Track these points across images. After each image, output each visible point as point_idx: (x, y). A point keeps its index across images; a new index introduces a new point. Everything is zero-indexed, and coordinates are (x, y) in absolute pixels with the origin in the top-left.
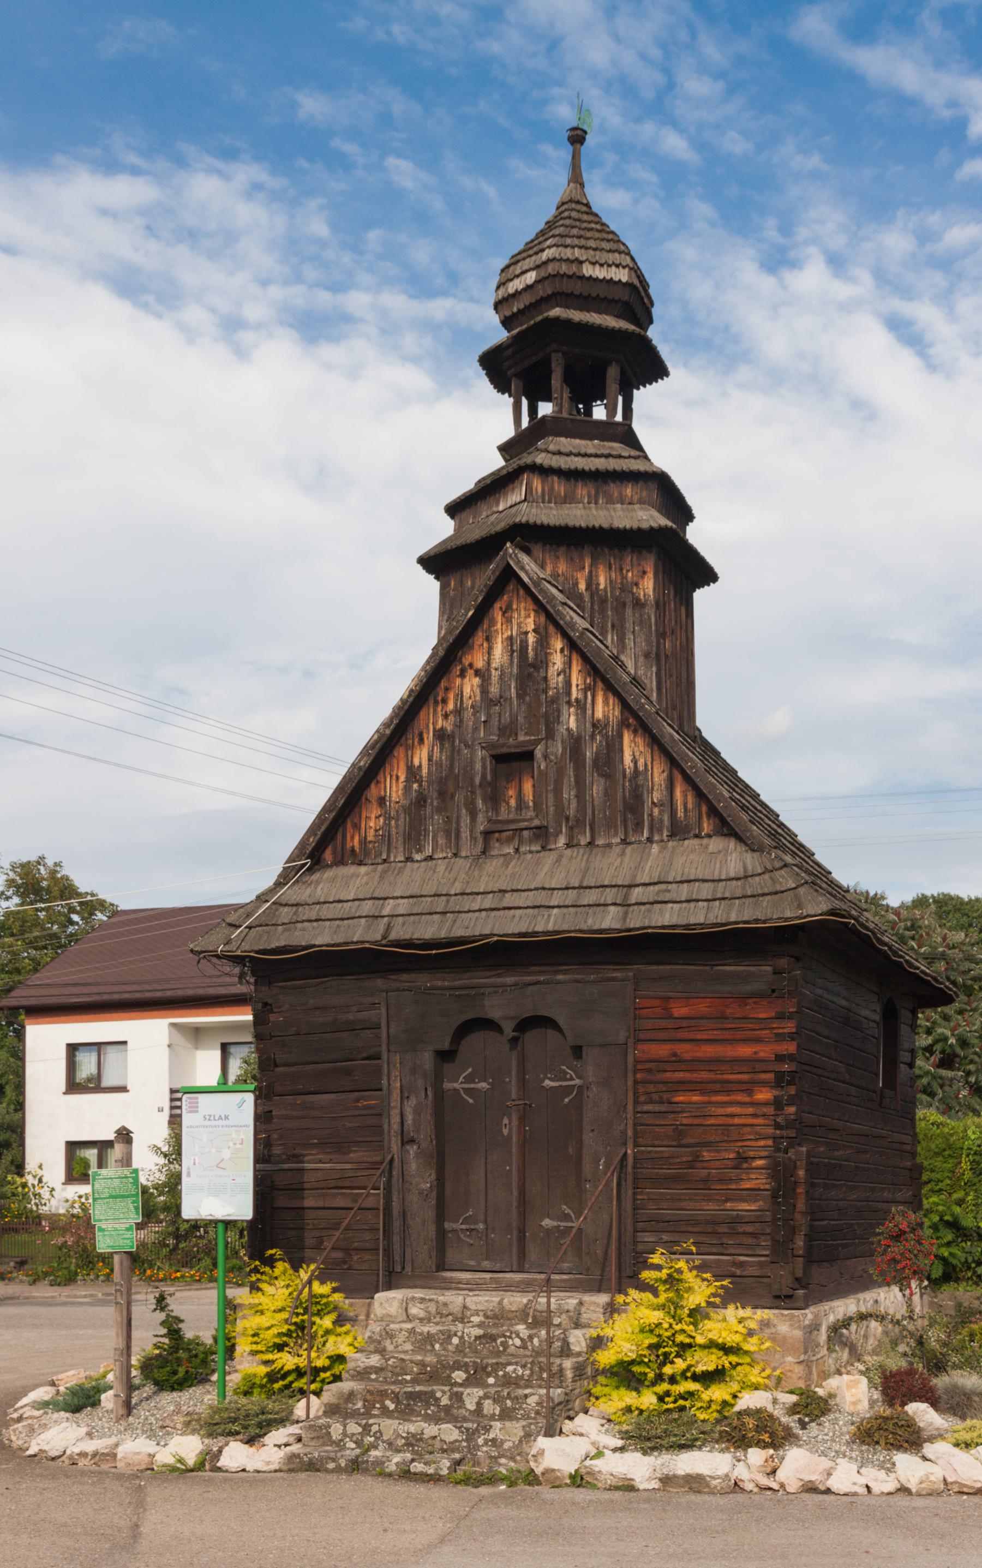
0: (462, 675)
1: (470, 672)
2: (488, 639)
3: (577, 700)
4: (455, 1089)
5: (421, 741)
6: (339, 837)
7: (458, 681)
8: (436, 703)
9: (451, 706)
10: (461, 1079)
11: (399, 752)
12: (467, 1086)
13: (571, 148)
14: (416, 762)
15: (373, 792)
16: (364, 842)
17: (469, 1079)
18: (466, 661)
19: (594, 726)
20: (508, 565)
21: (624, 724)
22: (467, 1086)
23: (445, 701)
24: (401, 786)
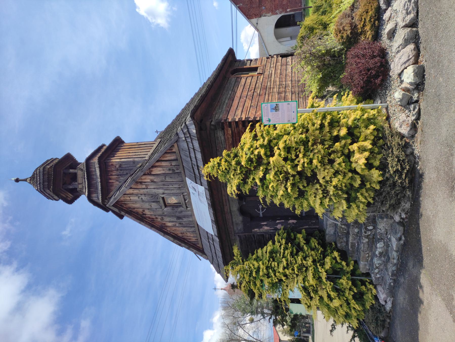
0: (145, 215)
1: (144, 212)
2: (134, 209)
3: (146, 186)
4: (262, 213)
5: (164, 224)
6: (194, 243)
7: (147, 216)
8: (154, 221)
9: (154, 217)
10: (259, 212)
11: (169, 229)
12: (261, 210)
13: (20, 182)
14: (171, 225)
15: (180, 235)
16: (194, 237)
17: (259, 210)
18: (141, 214)
19: (152, 182)
20: (112, 206)
21: (150, 174)
22: (261, 210)
23: (153, 219)
24: (177, 228)
